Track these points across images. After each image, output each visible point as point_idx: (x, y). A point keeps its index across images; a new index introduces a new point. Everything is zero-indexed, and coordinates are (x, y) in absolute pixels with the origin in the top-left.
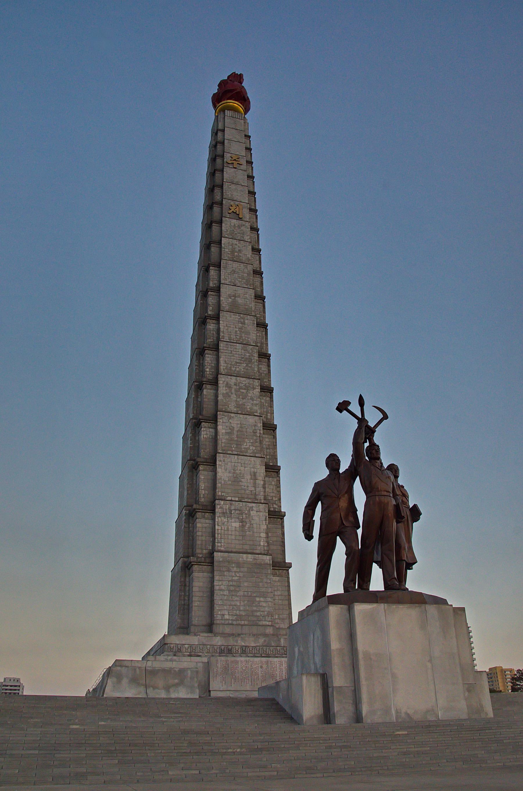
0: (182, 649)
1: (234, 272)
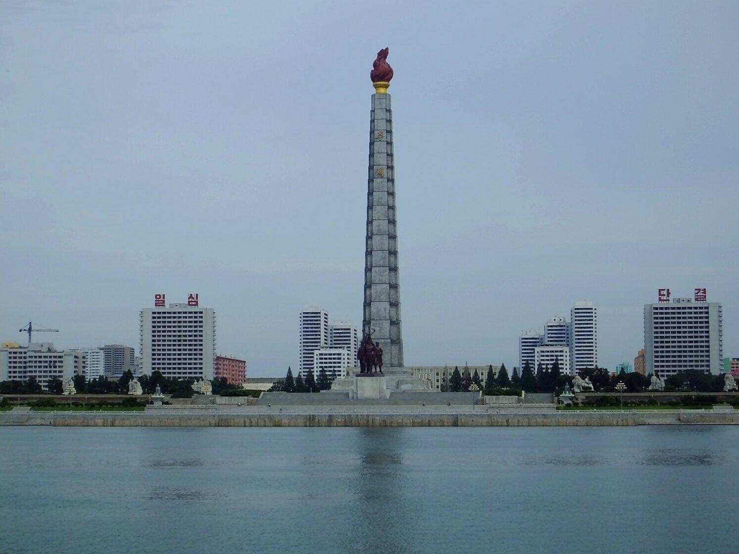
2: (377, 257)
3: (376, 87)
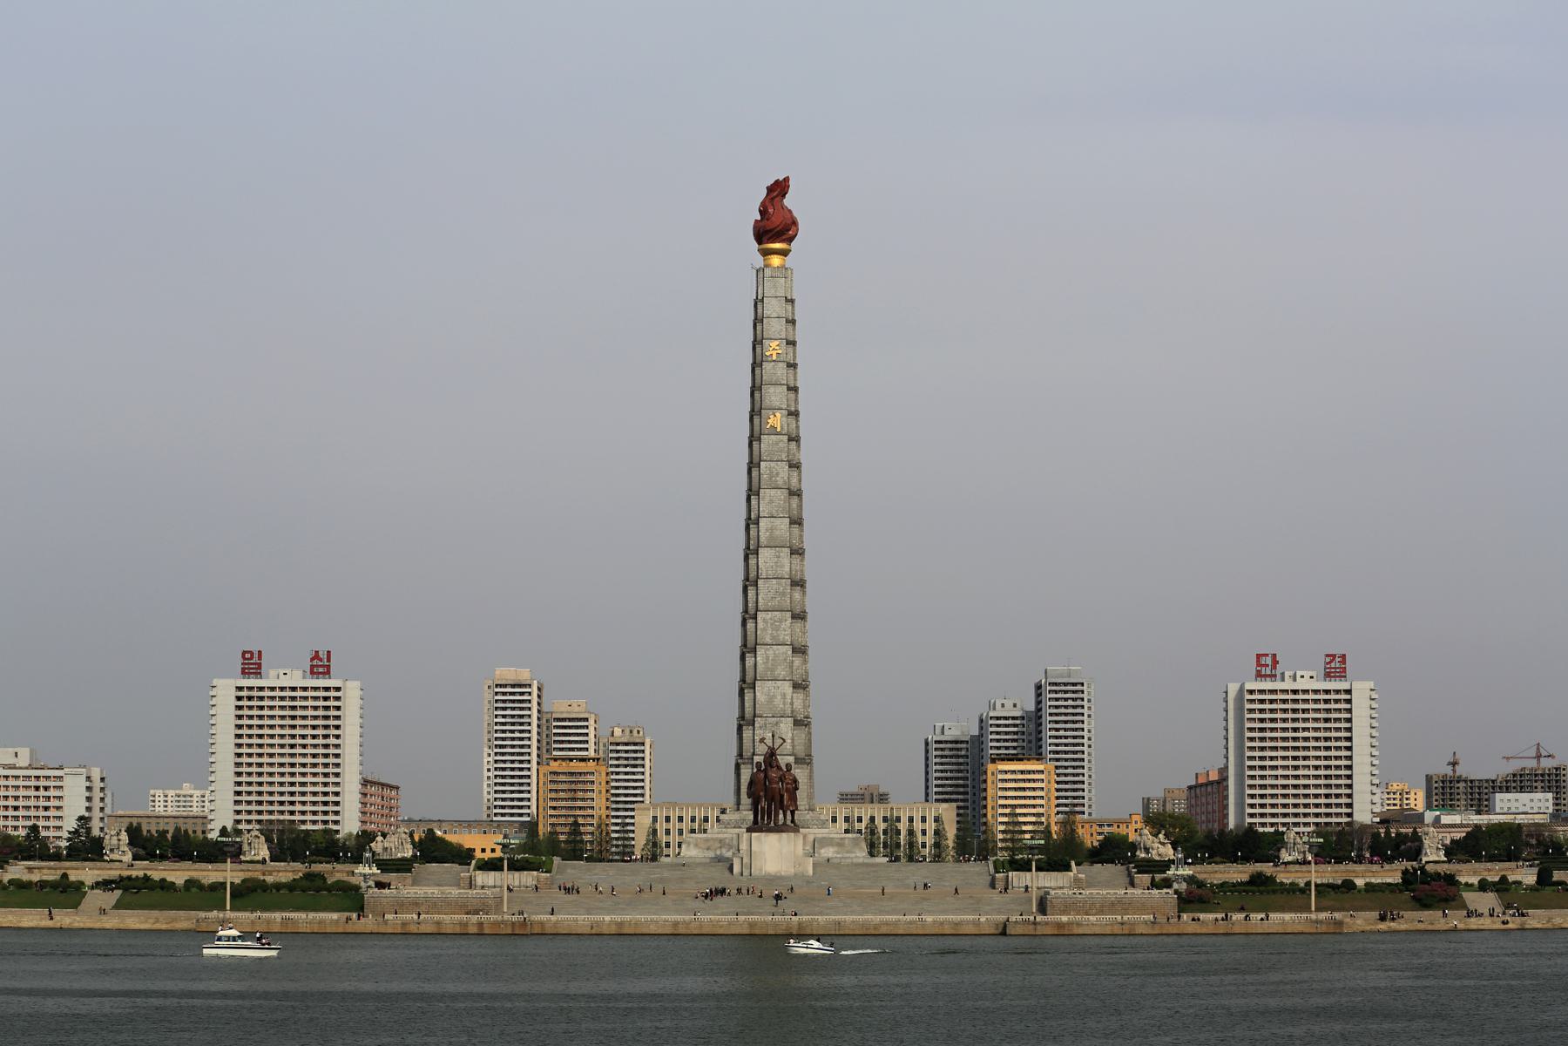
1: (771, 501)
2: (766, 592)
3: (766, 253)
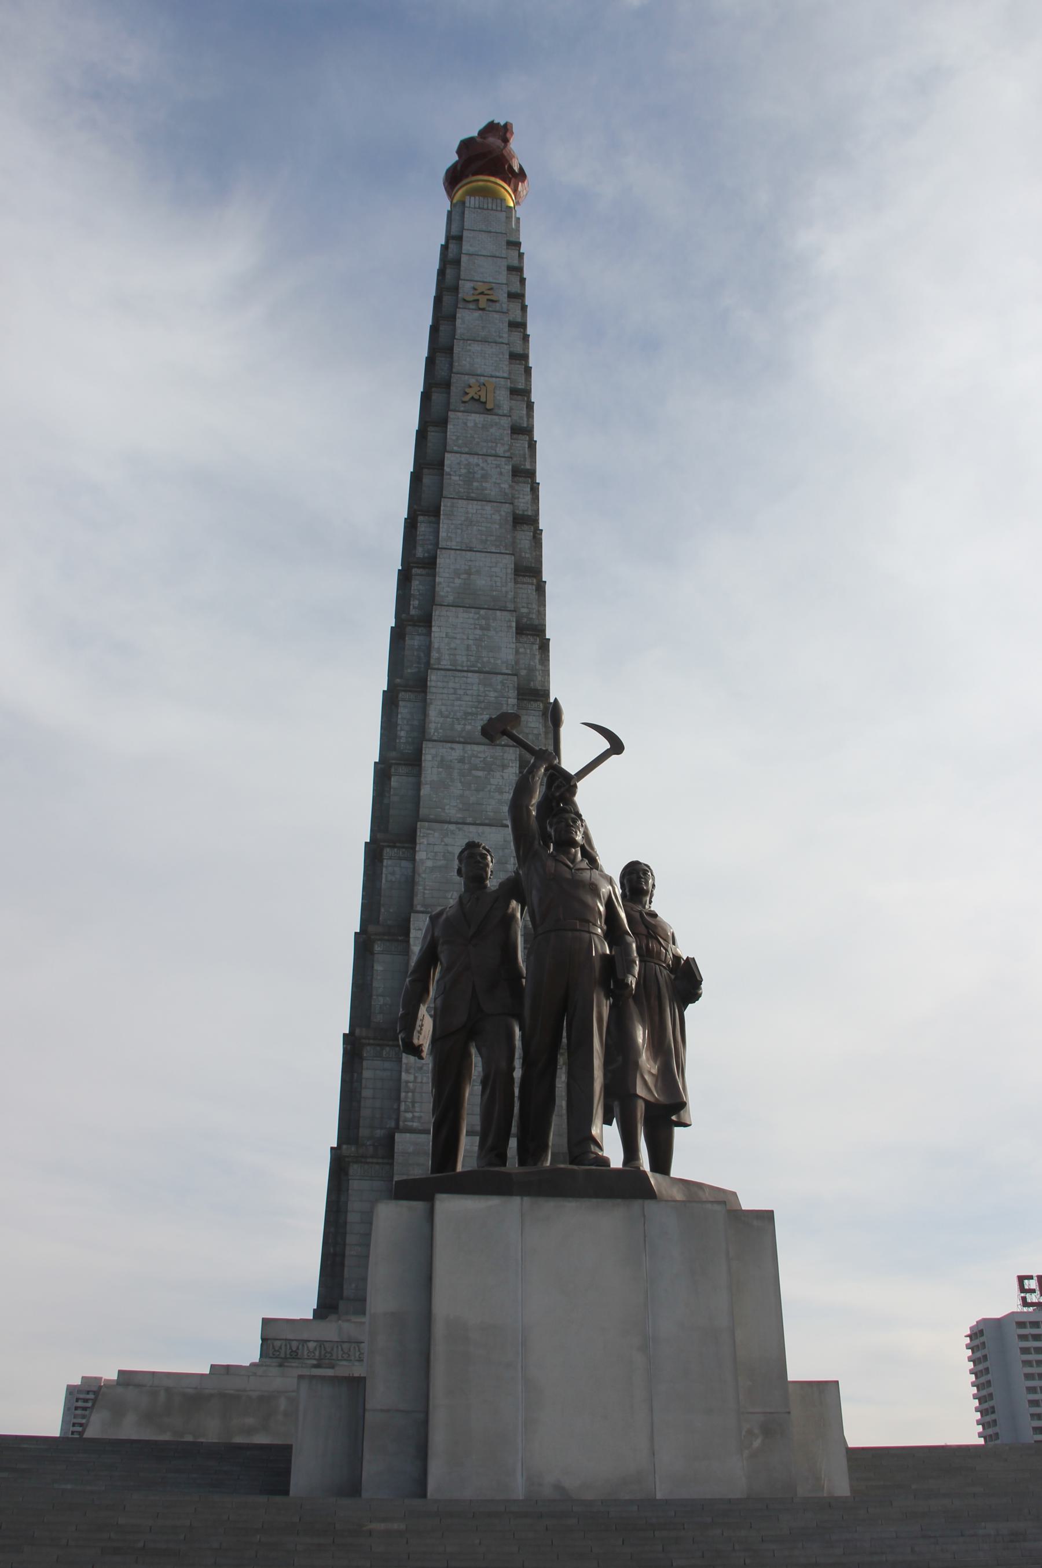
0: (300, 1352)
